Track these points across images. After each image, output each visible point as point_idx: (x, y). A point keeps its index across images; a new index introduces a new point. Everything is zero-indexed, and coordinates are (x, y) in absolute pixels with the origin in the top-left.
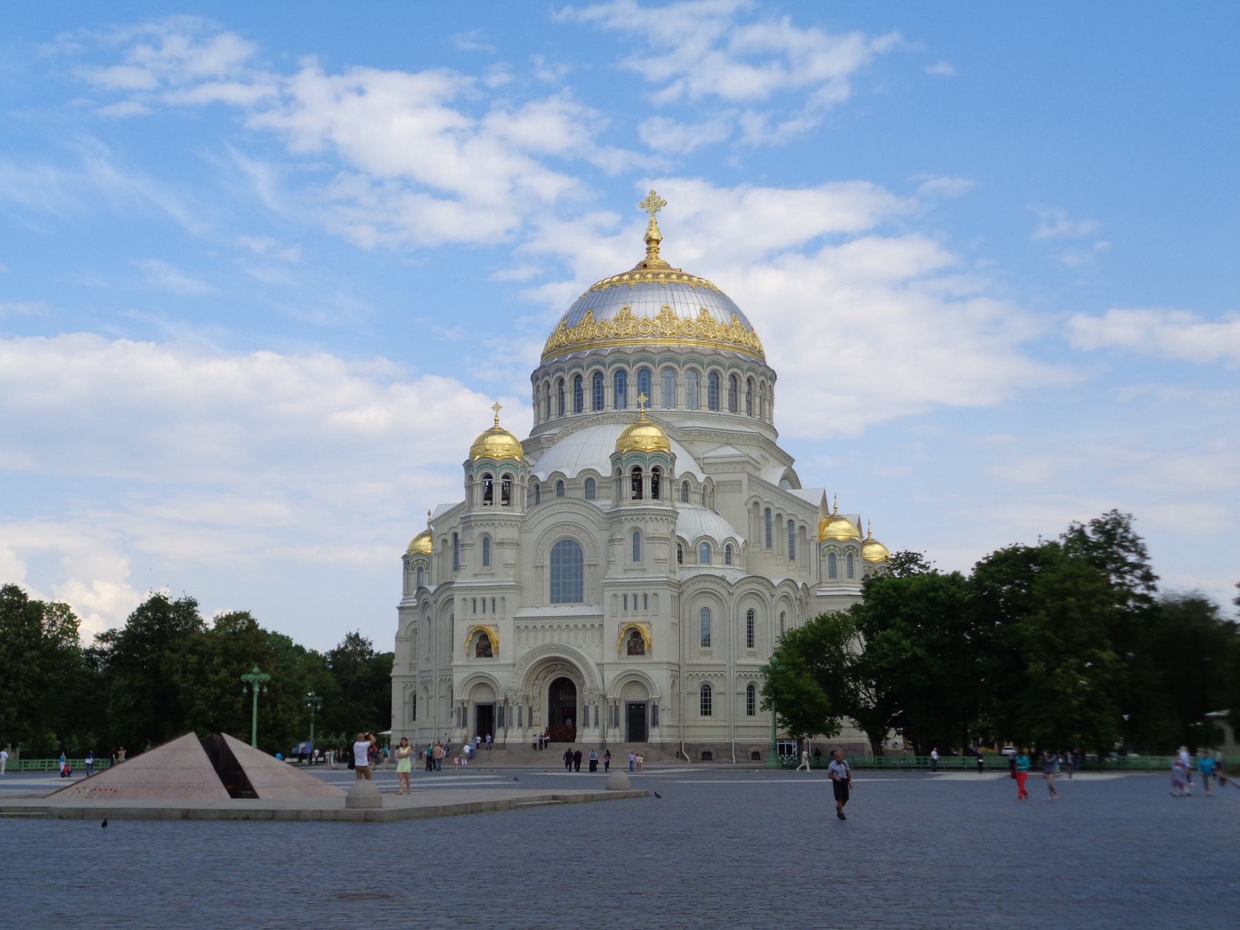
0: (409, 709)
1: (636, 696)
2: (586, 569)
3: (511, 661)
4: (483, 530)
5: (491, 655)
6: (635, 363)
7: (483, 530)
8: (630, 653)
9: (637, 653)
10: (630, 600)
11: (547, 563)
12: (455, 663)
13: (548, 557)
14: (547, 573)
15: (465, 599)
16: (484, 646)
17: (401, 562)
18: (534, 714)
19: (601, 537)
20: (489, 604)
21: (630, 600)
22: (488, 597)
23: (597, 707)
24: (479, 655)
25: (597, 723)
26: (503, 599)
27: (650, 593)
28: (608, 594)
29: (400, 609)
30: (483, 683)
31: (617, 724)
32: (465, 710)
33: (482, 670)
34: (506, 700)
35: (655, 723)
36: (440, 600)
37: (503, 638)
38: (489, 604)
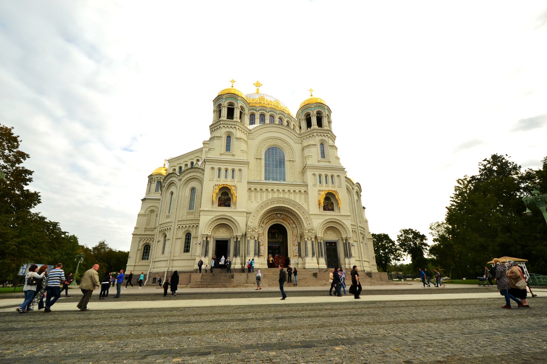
0: (140, 254)
1: (331, 237)
2: (287, 164)
3: (245, 210)
4: (227, 130)
5: (229, 206)
6: (269, 112)
7: (227, 130)
8: (325, 209)
9: (329, 210)
10: (323, 178)
11: (263, 157)
12: (202, 209)
13: (263, 153)
14: (263, 161)
15: (213, 168)
16: (225, 197)
17: (148, 179)
18: (261, 247)
19: (297, 148)
20: (230, 172)
21: (323, 178)
22: (230, 168)
23: (312, 242)
24: (220, 205)
25: (313, 254)
26: (240, 170)
27: (335, 175)
28: (309, 173)
29: (143, 200)
30: (224, 224)
31: (322, 256)
32: (207, 242)
33: (224, 214)
34: (245, 235)
35: (348, 255)
36: (183, 179)
37: (240, 195)
38: (230, 172)
